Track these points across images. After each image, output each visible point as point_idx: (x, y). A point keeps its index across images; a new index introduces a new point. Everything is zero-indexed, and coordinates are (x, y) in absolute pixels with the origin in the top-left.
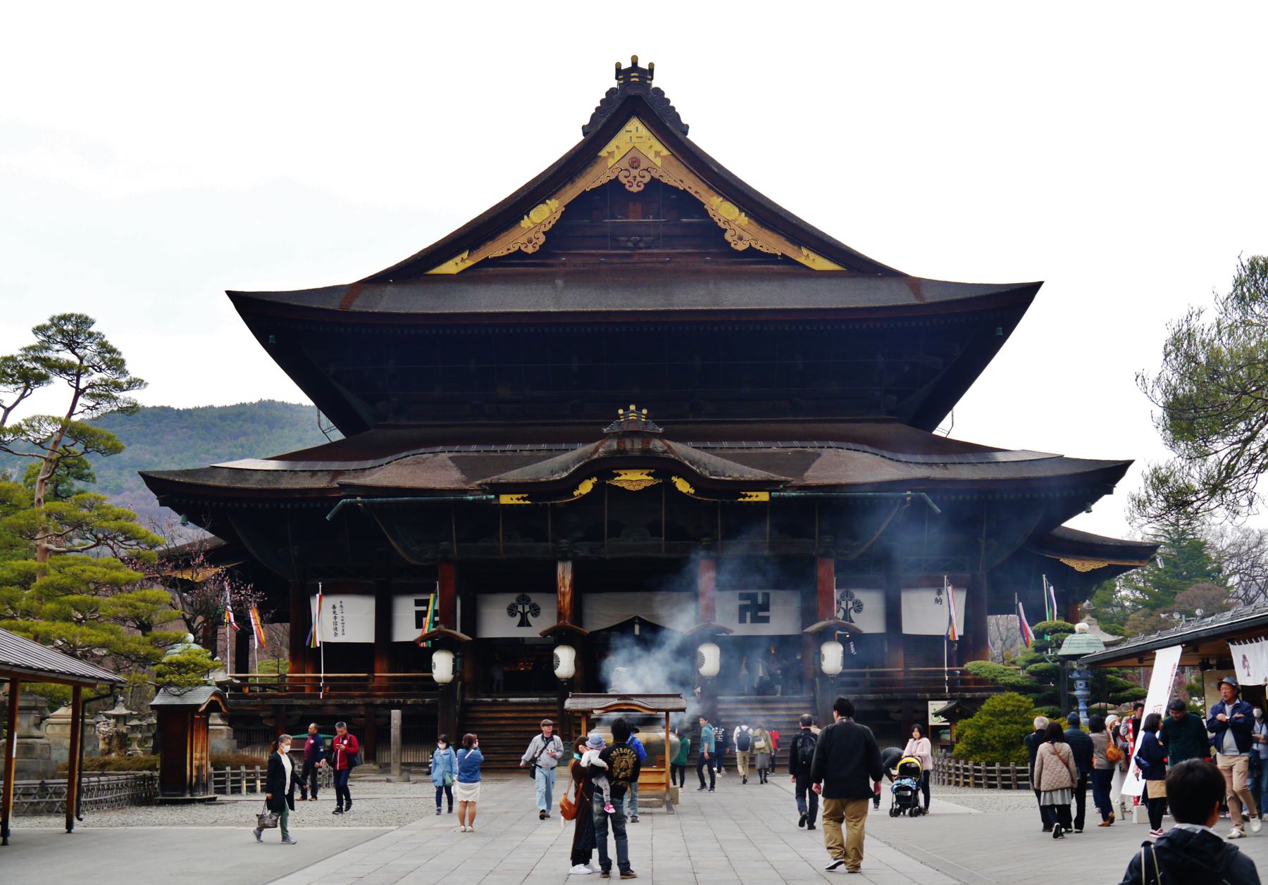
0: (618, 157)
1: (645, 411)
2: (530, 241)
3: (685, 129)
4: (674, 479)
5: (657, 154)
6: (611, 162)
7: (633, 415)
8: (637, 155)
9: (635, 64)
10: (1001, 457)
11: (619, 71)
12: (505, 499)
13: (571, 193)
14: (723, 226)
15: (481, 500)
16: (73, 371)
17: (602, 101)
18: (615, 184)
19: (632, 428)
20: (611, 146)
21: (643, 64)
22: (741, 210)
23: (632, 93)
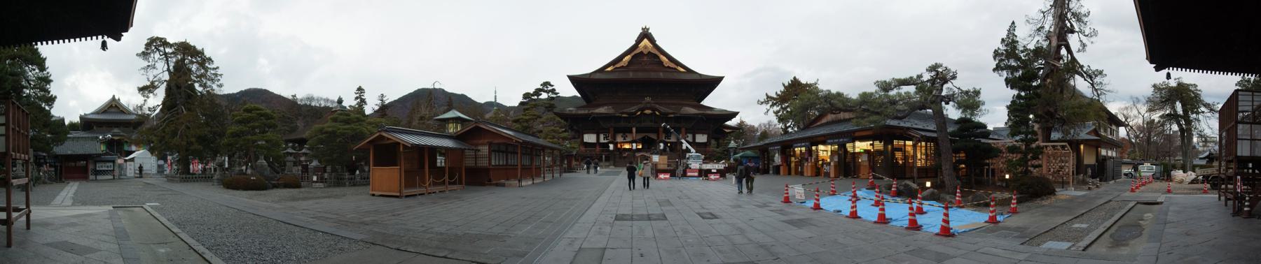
7: (648, 99)
16: (547, 92)
18: (642, 53)
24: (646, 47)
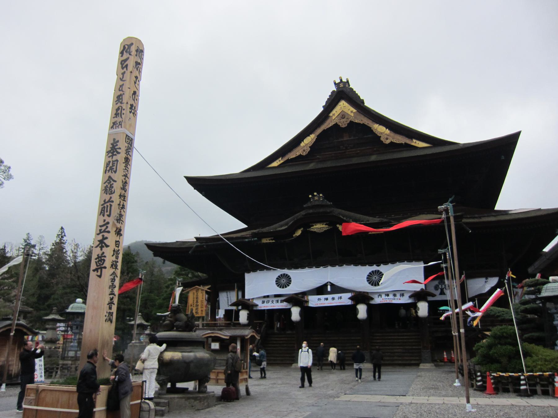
0: (336, 115)
1: (321, 195)
2: (304, 151)
3: (363, 102)
4: (338, 226)
5: (352, 112)
6: (334, 118)
8: (343, 113)
9: (341, 80)
10: (510, 212)
11: (335, 83)
12: (265, 241)
13: (319, 131)
14: (379, 135)
15: (251, 241)
17: (330, 96)
18: (336, 125)
19: (317, 203)
20: (334, 112)
21: (344, 80)
22: (386, 128)
23: (340, 89)
24: (343, 115)
